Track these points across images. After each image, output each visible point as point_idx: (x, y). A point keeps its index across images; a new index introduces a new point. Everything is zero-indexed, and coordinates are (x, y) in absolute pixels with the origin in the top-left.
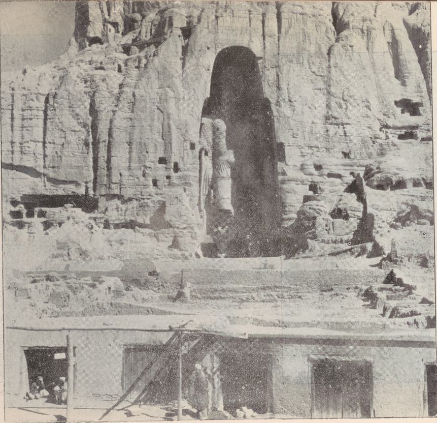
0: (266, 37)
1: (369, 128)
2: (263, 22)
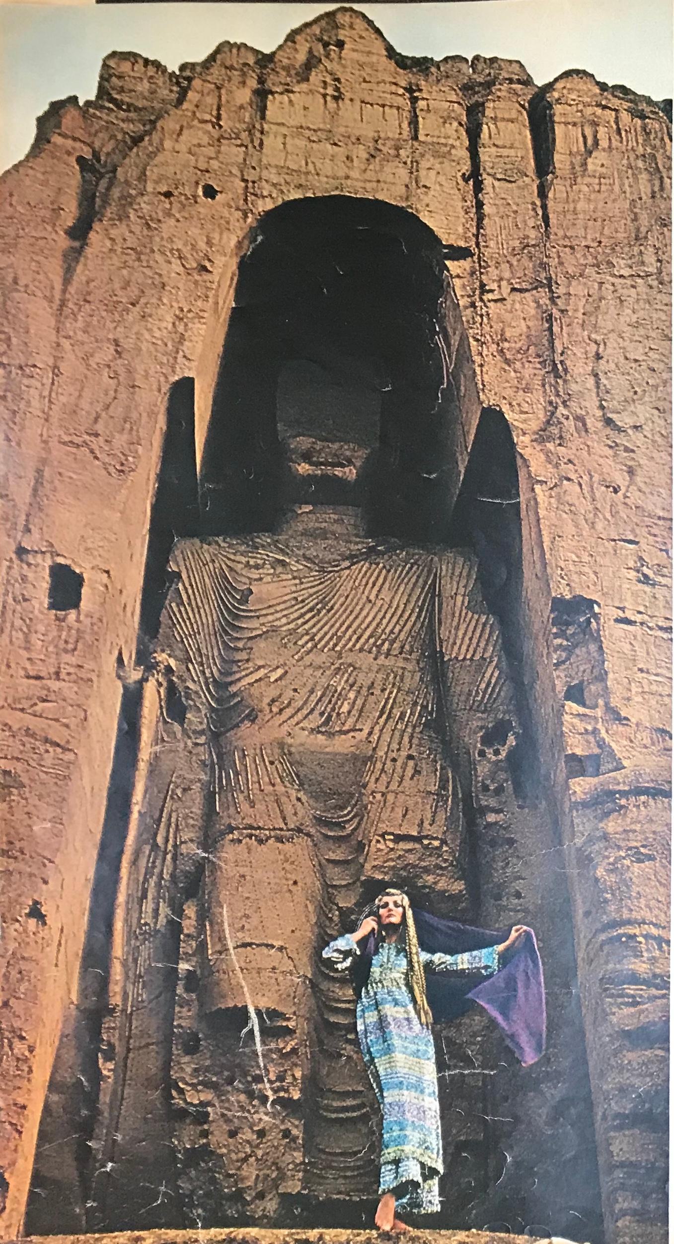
0: (488, 181)
2: (474, 133)
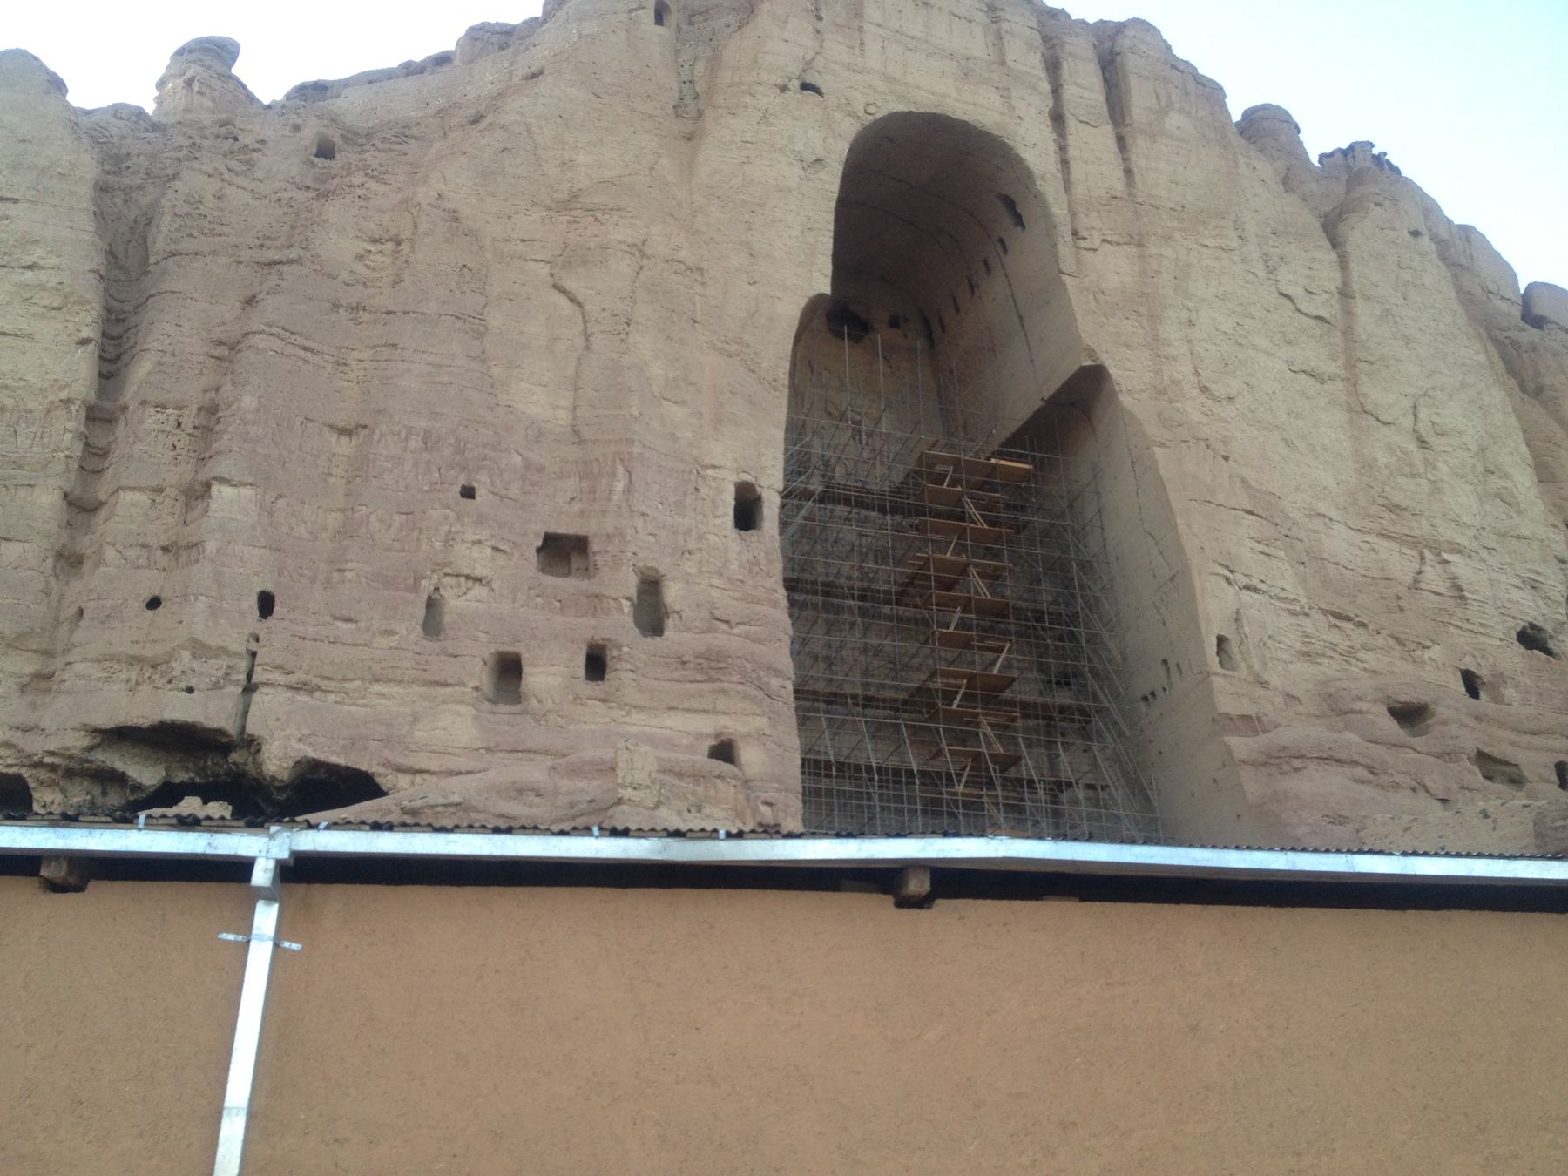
0: (1071, 124)
1: (1535, 586)
